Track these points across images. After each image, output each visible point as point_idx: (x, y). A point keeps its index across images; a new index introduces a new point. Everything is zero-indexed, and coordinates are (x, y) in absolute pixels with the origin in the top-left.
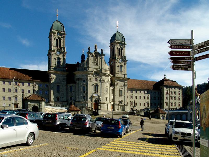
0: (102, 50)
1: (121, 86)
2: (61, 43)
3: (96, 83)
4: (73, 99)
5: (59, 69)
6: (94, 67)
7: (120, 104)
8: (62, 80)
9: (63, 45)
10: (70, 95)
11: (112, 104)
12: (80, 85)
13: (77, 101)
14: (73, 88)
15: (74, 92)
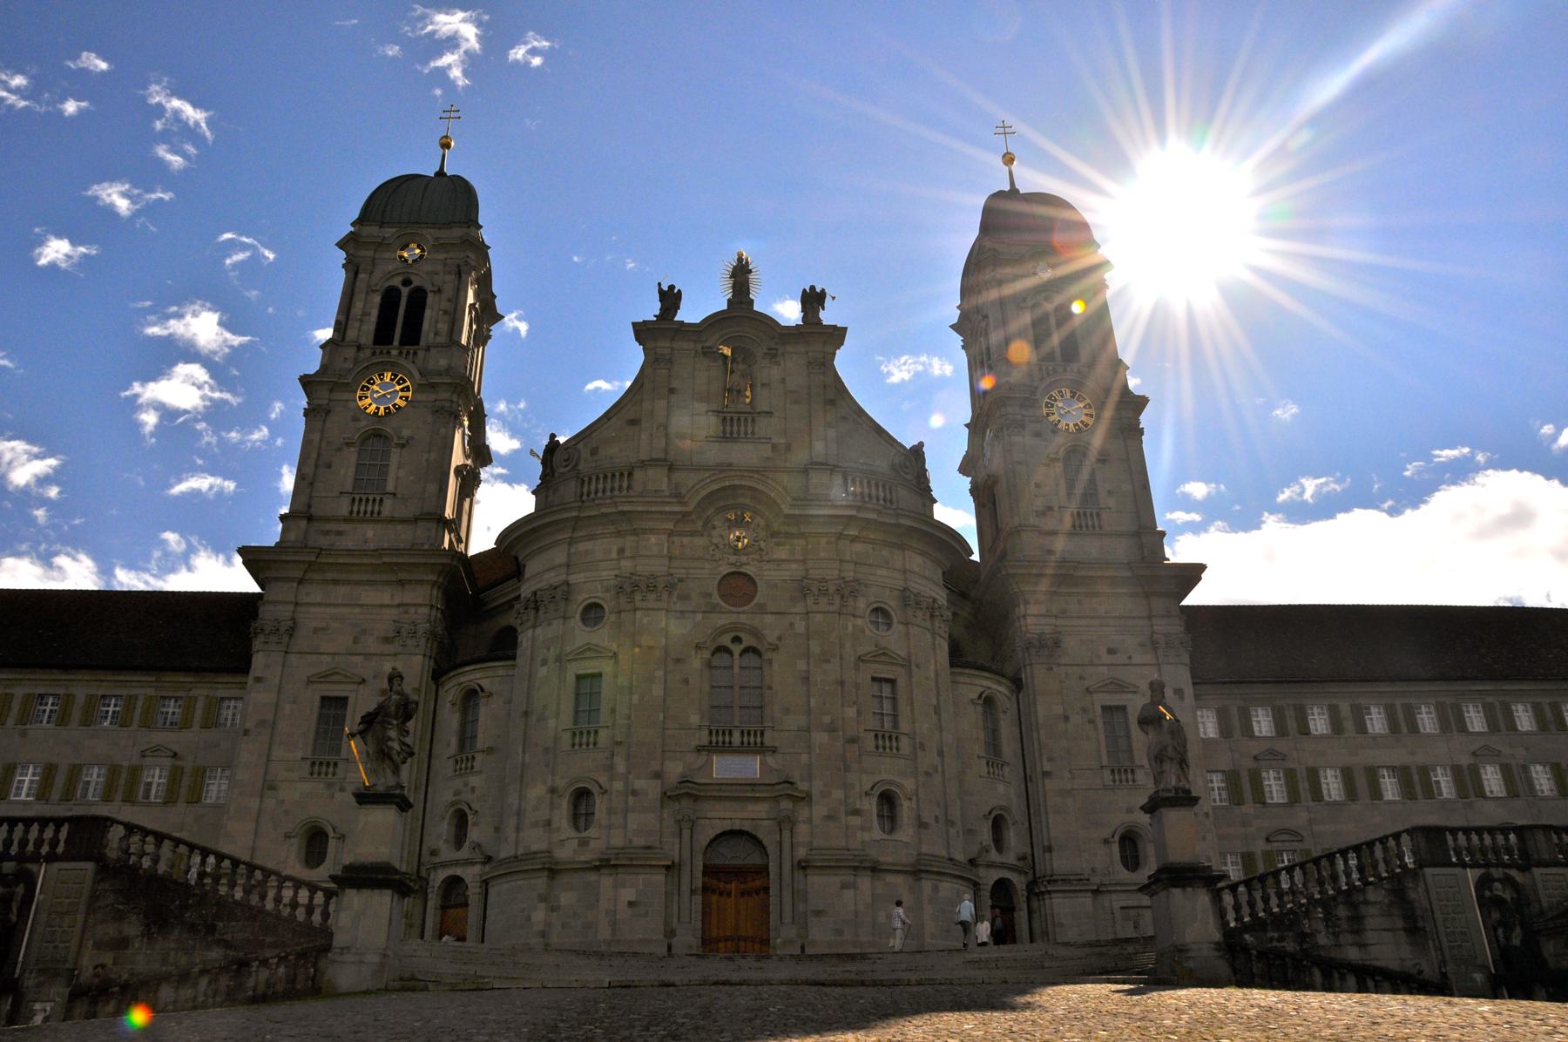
0: (813, 300)
1: (1107, 659)
2: (428, 313)
3: (743, 618)
4: (474, 834)
5: (370, 534)
6: (714, 454)
7: (1123, 874)
8: (387, 640)
9: (443, 327)
10: (449, 797)
11: (995, 875)
12: (544, 662)
13: (505, 852)
14: (486, 712)
15: (490, 751)
